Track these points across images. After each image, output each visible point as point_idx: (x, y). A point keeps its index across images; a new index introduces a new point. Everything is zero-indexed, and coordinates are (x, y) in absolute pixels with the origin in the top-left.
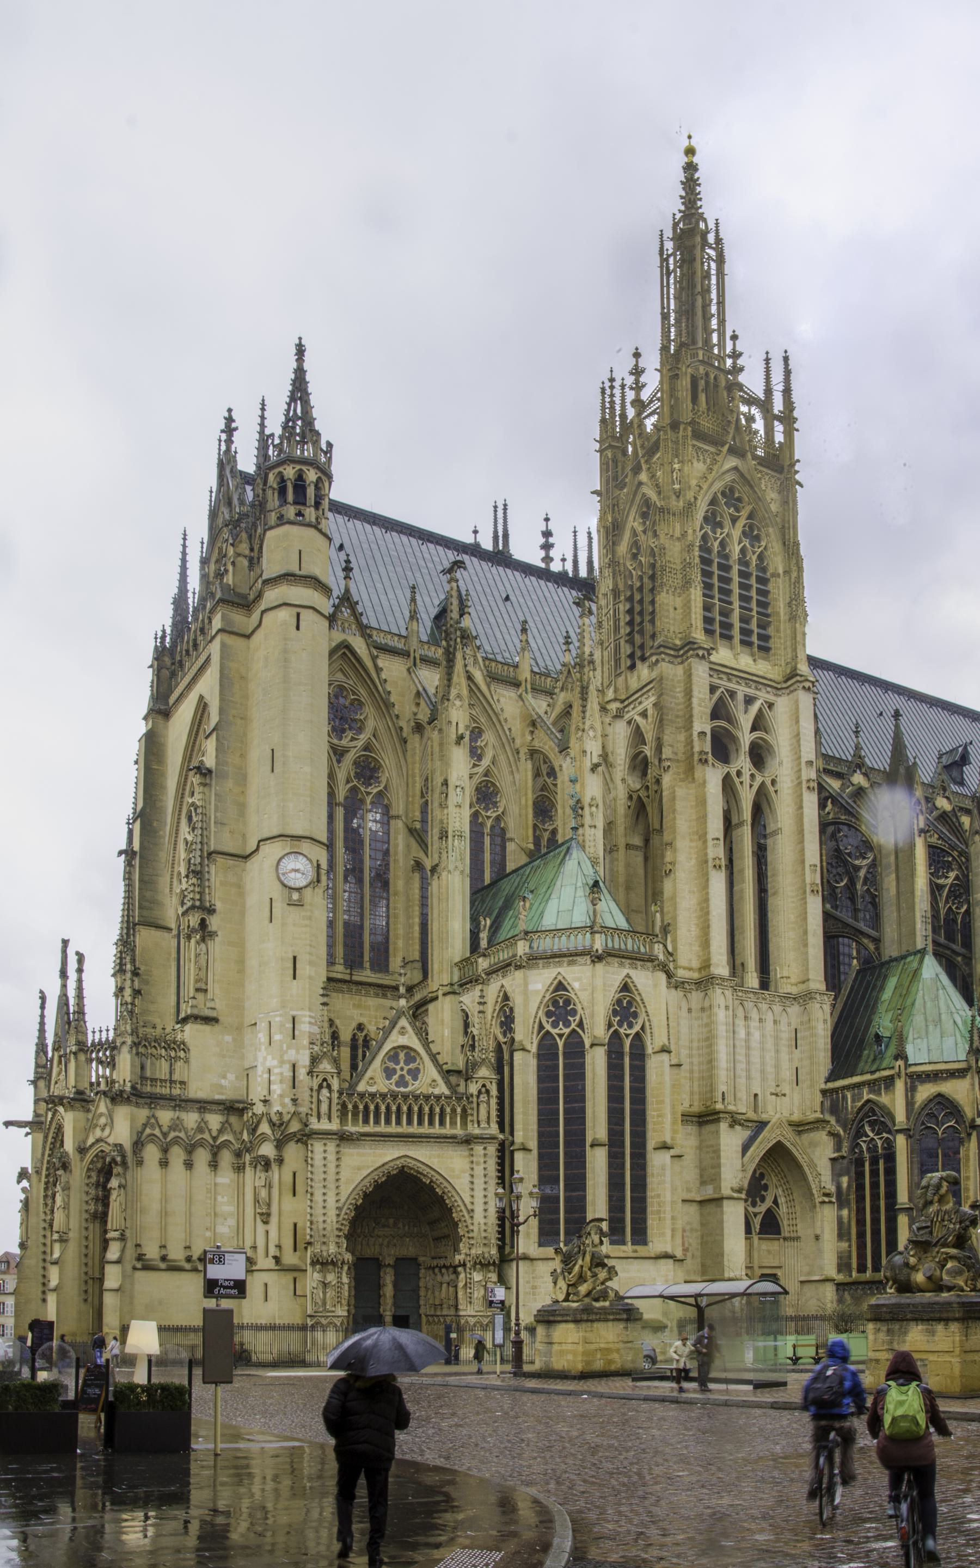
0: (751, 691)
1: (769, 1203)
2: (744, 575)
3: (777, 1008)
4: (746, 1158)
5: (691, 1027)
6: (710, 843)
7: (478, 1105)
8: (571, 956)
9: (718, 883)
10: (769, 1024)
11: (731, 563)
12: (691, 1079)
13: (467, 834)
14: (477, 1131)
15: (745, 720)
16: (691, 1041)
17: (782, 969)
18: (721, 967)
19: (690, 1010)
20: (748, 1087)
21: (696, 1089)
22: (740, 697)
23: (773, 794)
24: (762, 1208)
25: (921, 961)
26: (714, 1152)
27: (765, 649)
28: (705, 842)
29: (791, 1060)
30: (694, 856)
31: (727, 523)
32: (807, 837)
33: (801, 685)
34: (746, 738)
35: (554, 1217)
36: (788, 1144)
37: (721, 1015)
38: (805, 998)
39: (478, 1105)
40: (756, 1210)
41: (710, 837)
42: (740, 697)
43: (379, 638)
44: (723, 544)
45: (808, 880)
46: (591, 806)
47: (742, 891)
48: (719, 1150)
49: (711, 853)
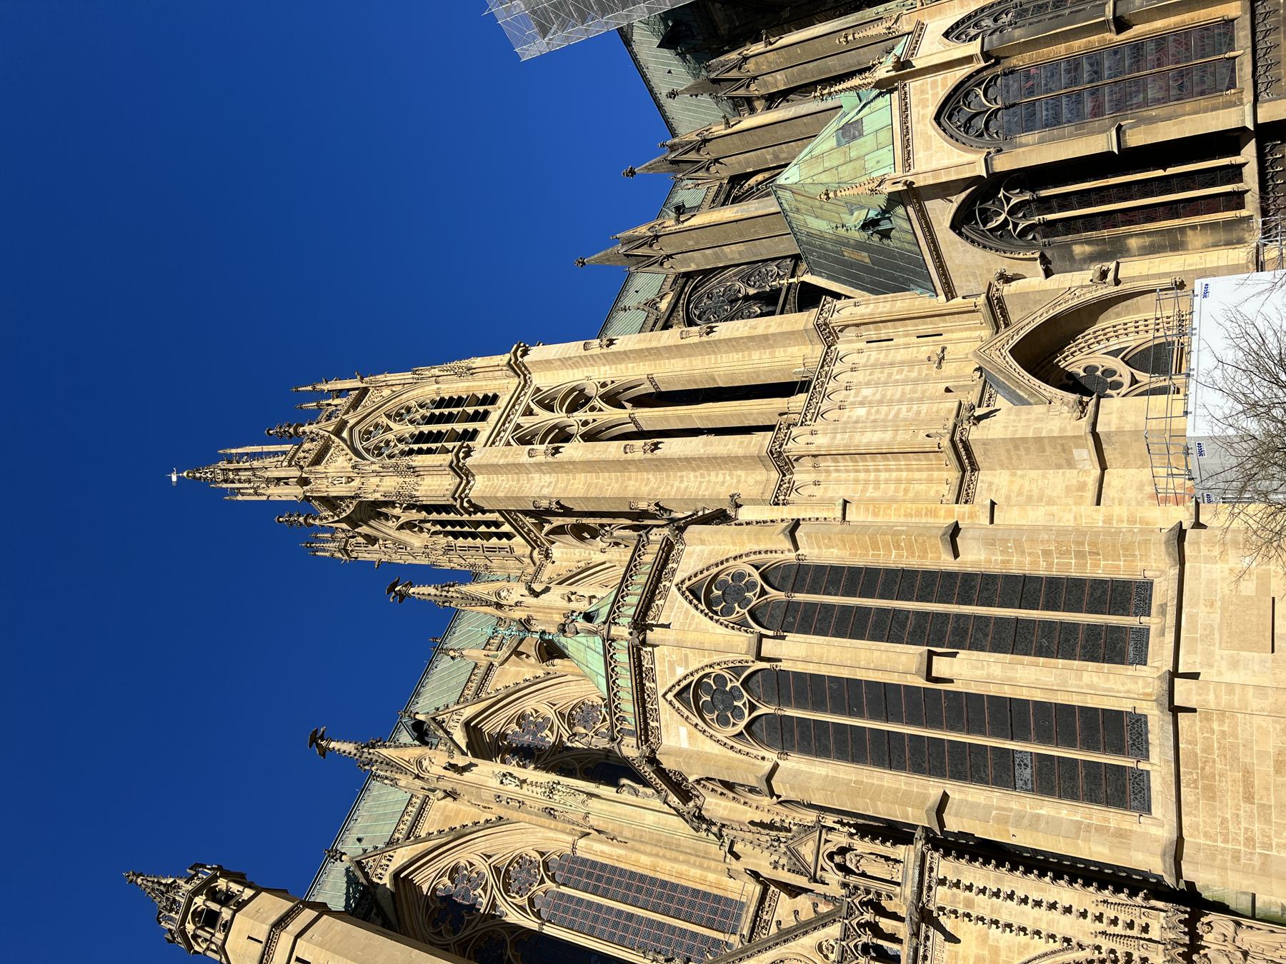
0: (520, 409)
1: (1116, 363)
2: (431, 420)
3: (837, 368)
4: (1032, 401)
5: (838, 481)
6: (629, 456)
7: (864, 875)
8: (640, 674)
9: (671, 447)
10: (859, 377)
11: (417, 432)
12: (910, 481)
13: (553, 777)
14: (909, 890)
15: (544, 418)
16: (857, 481)
17: (795, 366)
18: (762, 441)
19: (816, 483)
20: (932, 399)
21: (924, 475)
22: (522, 420)
23: (614, 385)
24: (1124, 372)
25: (781, 187)
26: (1017, 448)
27: (495, 397)
28: (626, 461)
29: (907, 346)
30: (645, 475)
31: (390, 436)
32: (654, 344)
33: (520, 359)
34: (559, 417)
35: (1081, 772)
36: (1017, 338)
37: (821, 441)
38: (828, 334)
39: (864, 875)
40: (1126, 380)
41: (624, 457)
42: (522, 420)
43: (404, 828)
44: (400, 440)
45: (696, 339)
46: (570, 600)
47: (700, 418)
48: (1013, 440)
49: (639, 455)
